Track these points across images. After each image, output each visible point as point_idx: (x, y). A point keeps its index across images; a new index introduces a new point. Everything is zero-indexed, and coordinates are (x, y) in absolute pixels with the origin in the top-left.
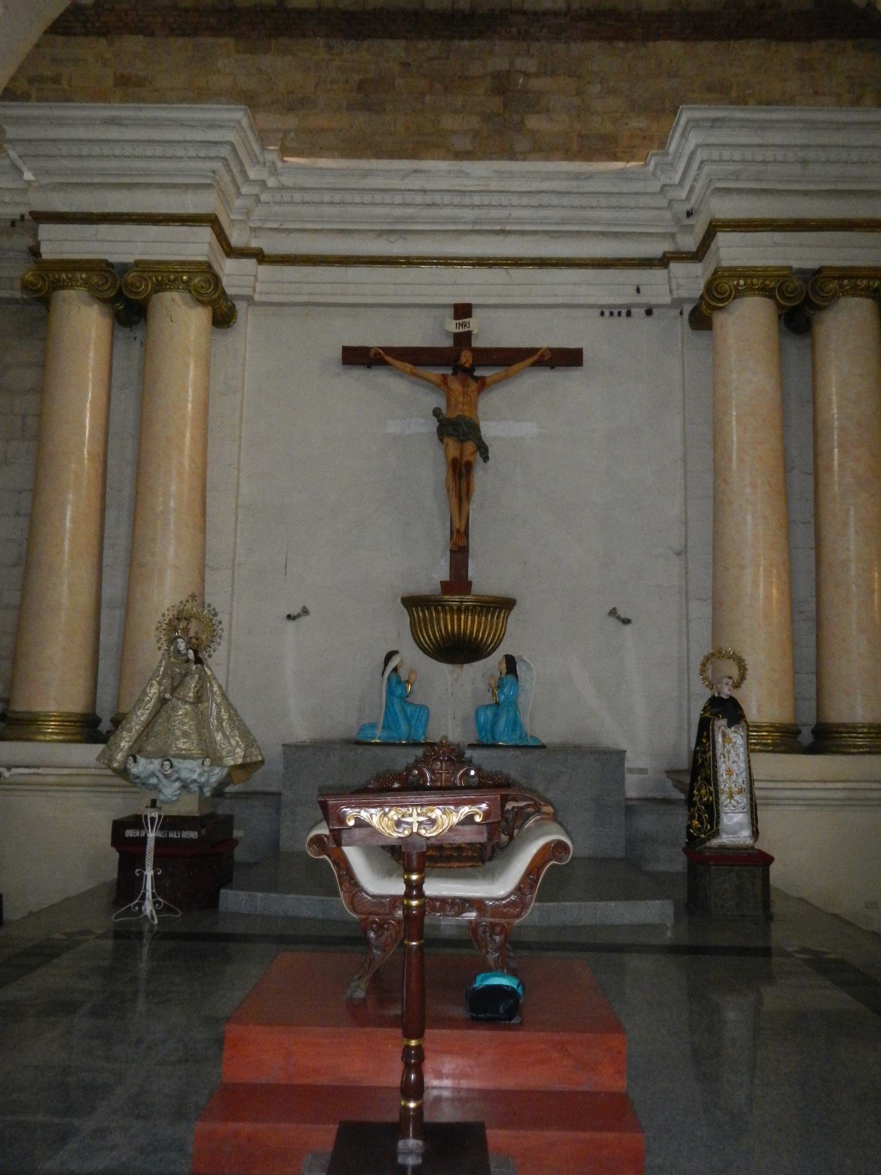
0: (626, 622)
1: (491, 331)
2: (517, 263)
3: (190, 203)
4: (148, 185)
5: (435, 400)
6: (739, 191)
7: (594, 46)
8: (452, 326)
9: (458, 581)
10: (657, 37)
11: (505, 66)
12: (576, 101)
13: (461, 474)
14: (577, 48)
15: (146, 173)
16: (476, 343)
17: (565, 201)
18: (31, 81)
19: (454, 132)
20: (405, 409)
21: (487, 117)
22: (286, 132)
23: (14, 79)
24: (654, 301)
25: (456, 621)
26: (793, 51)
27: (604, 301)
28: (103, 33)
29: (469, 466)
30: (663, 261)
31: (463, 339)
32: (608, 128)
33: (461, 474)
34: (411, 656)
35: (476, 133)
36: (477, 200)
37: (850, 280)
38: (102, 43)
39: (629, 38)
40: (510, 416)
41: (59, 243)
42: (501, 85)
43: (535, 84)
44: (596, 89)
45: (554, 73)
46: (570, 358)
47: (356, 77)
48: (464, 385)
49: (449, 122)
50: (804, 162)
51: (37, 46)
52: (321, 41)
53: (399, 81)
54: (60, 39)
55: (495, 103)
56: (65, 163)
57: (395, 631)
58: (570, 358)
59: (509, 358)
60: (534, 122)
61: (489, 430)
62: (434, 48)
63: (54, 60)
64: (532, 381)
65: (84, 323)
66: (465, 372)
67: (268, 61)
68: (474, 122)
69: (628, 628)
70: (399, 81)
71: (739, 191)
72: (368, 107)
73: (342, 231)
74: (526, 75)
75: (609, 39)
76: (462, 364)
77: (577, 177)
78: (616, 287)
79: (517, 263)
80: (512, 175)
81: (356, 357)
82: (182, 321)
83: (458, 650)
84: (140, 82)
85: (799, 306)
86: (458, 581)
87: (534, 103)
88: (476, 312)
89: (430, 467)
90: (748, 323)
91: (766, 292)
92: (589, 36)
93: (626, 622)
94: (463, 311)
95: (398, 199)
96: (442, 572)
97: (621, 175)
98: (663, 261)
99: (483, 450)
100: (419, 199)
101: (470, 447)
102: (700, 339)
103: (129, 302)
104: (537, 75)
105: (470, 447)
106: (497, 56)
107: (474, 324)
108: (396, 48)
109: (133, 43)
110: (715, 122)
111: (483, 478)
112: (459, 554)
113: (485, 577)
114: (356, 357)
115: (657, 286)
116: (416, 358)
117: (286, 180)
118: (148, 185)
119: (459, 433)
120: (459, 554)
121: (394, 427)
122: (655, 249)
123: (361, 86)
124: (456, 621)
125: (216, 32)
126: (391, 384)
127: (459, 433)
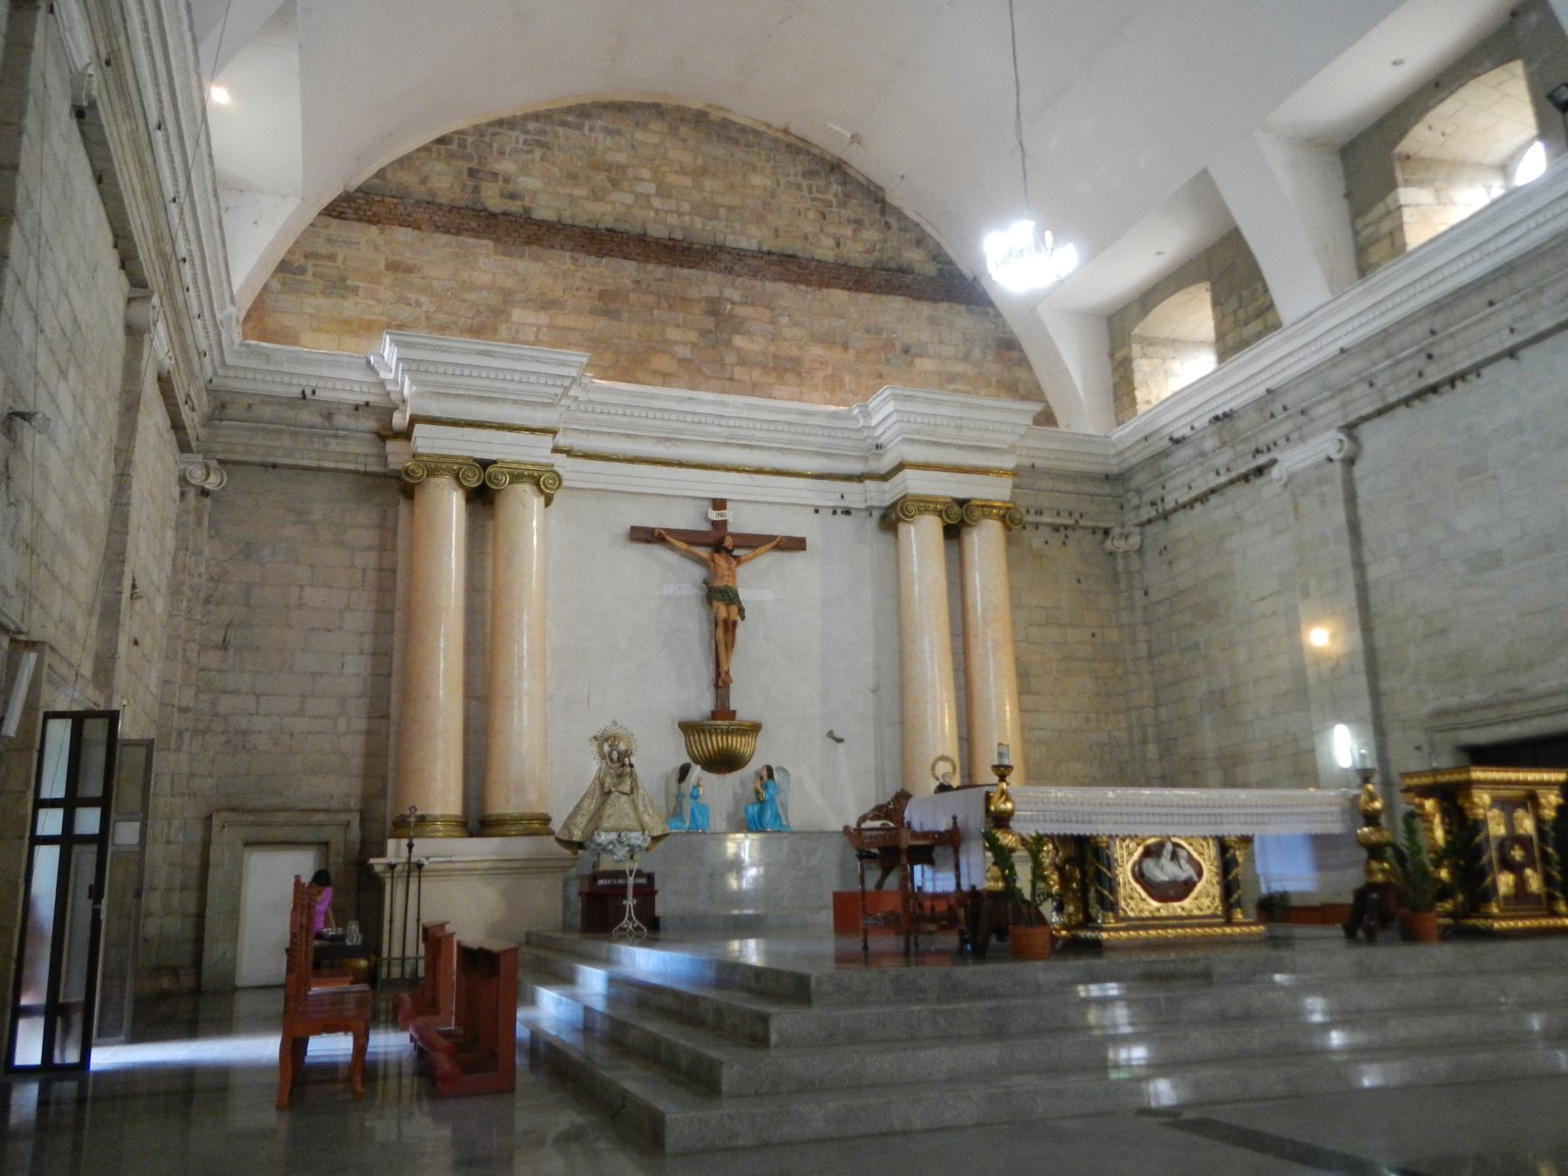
0: (840, 741)
1: (740, 521)
2: (759, 471)
3: (539, 418)
4: (505, 400)
5: (697, 573)
6: (919, 442)
7: (783, 287)
8: (714, 515)
9: (723, 711)
10: (828, 286)
11: (717, 294)
12: (771, 328)
14: (770, 286)
15: (504, 390)
16: (730, 529)
17: (793, 429)
18: (306, 256)
19: (678, 343)
20: (679, 579)
21: (704, 333)
22: (539, 327)
23: (289, 252)
24: (852, 505)
25: (717, 741)
26: (925, 308)
27: (817, 503)
28: (374, 220)
29: (735, 624)
30: (860, 478)
31: (720, 525)
32: (795, 352)
35: (694, 345)
36: (731, 423)
37: (986, 508)
38: (374, 230)
39: (808, 283)
41: (427, 440)
42: (714, 308)
43: (740, 311)
44: (785, 320)
45: (753, 304)
46: (797, 544)
47: (597, 288)
48: (728, 561)
49: (673, 334)
50: (961, 427)
51: (312, 225)
52: (568, 254)
53: (632, 296)
54: (335, 222)
55: (709, 323)
56: (440, 378)
58: (797, 544)
59: (754, 542)
60: (738, 341)
61: (744, 595)
63: (329, 240)
64: (767, 560)
65: (451, 505)
66: (718, 547)
67: (523, 265)
68: (693, 336)
69: (840, 745)
70: (632, 296)
71: (919, 442)
72: (608, 314)
73: (629, 436)
74: (733, 303)
75: (795, 282)
76: (717, 544)
77: (803, 413)
78: (828, 494)
79: (759, 471)
80: (758, 408)
81: (645, 536)
83: (725, 762)
84: (409, 270)
87: (738, 326)
88: (729, 505)
89: (694, 625)
90: (923, 535)
91: (940, 514)
92: (779, 278)
93: (840, 741)
94: (719, 504)
95: (674, 417)
97: (834, 415)
98: (860, 478)
99: (741, 611)
100: (689, 418)
101: (734, 609)
102: (888, 537)
104: (741, 304)
105: (734, 609)
106: (707, 284)
107: (729, 514)
108: (629, 269)
109: (402, 234)
110: (907, 398)
114: (645, 536)
115: (855, 495)
116: (690, 538)
117: (592, 396)
118: (505, 400)
119: (721, 601)
121: (668, 590)
122: (856, 467)
123: (602, 295)
124: (717, 741)
125: (476, 233)
127: (721, 601)
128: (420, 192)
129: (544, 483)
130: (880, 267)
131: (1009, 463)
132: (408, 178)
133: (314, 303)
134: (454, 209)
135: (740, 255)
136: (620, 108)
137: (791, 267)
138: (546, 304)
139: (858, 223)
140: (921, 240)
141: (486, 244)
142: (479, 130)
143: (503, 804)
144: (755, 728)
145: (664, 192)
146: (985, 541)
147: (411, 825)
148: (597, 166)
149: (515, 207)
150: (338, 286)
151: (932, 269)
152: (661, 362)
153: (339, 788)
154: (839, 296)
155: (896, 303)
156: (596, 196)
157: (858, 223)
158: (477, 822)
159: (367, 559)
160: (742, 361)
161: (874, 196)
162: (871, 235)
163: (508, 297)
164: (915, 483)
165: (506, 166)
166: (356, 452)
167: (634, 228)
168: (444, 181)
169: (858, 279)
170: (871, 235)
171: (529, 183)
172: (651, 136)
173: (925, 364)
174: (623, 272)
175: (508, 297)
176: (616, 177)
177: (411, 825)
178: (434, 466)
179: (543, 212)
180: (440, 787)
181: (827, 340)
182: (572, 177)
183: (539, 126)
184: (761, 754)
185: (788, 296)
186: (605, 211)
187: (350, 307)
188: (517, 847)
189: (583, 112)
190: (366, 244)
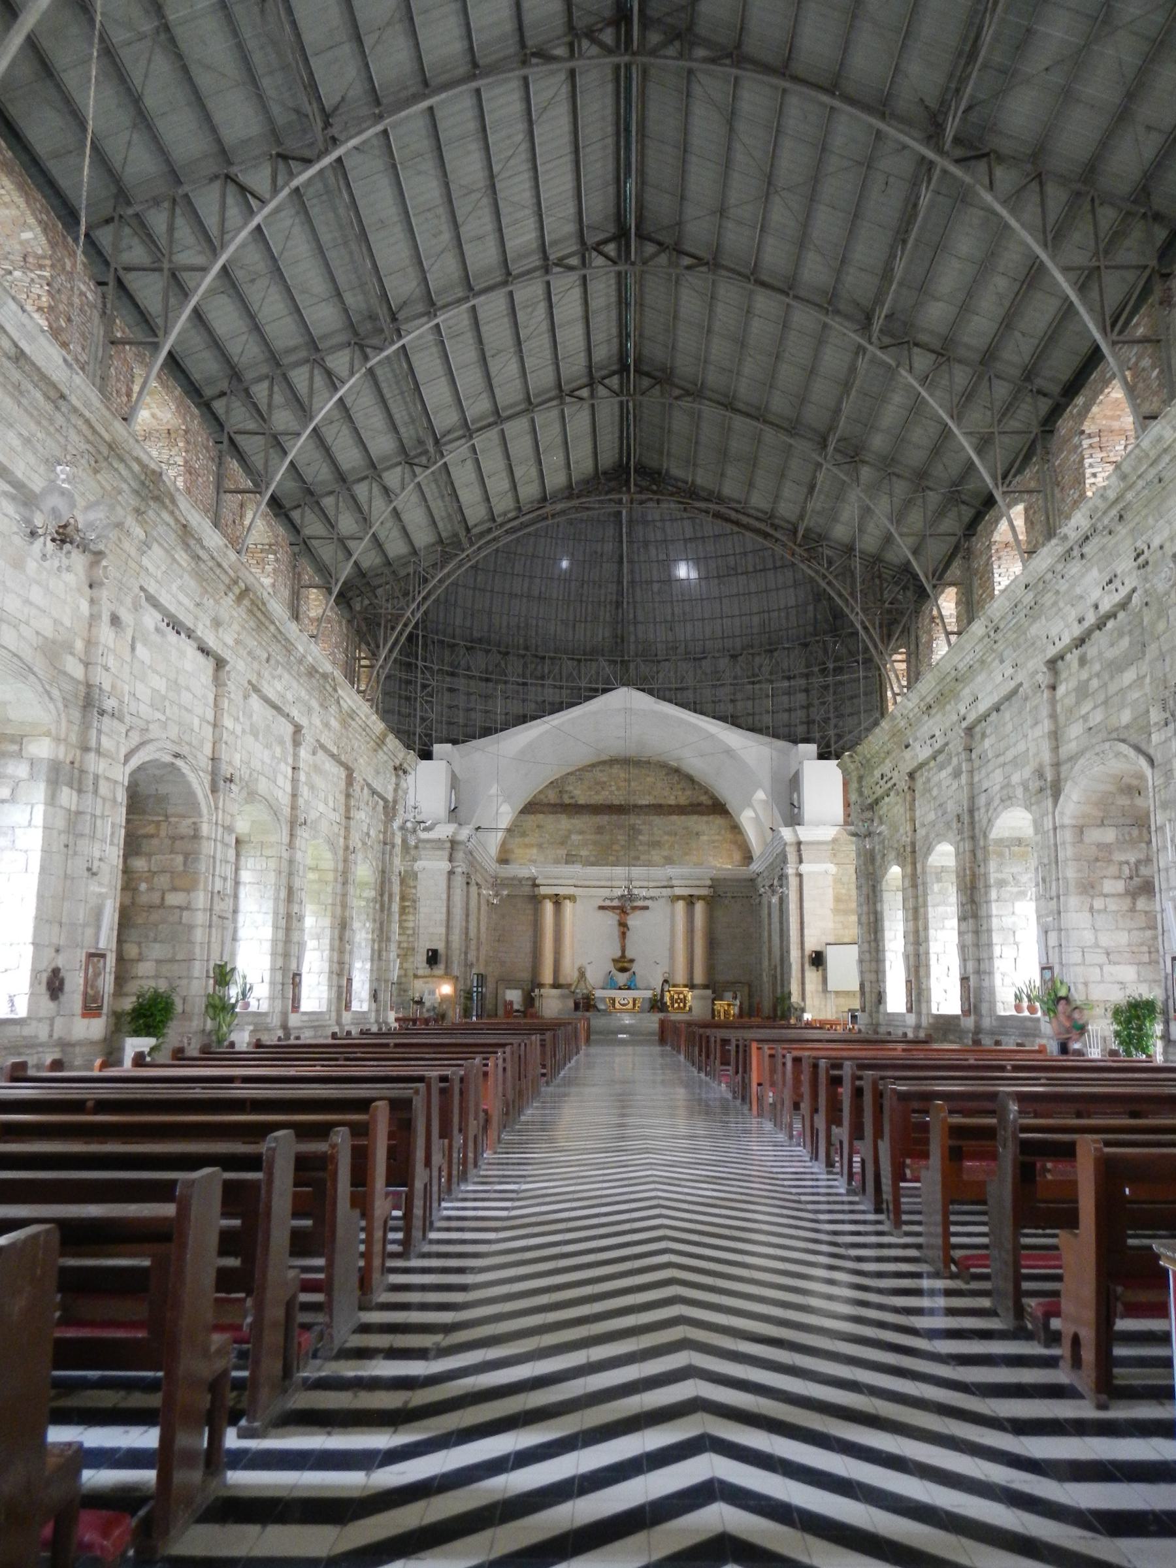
9: (623, 956)
13: (624, 934)
20: (611, 919)
25: (623, 964)
26: (705, 818)
33: (624, 934)
34: (614, 972)
37: (699, 898)
40: (634, 920)
41: (544, 890)
42: (632, 827)
57: (610, 966)
58: (646, 908)
62: (615, 817)
65: (549, 907)
81: (601, 908)
82: (568, 906)
83: (623, 970)
85: (690, 900)
86: (623, 956)
87: (640, 832)
89: (616, 931)
90: (681, 905)
96: (619, 954)
103: (557, 900)
108: (606, 818)
111: (628, 934)
112: (623, 951)
113: (629, 954)
114: (601, 908)
116: (614, 908)
119: (623, 925)
120: (623, 951)
124: (623, 964)
126: (610, 913)
127: (623, 925)
128: (545, 801)
129: (572, 898)
130: (691, 805)
131: (709, 883)
132: (542, 796)
133: (518, 840)
134: (555, 805)
135: (641, 807)
136: (604, 763)
137: (659, 809)
138: (581, 833)
139: (684, 789)
140: (707, 792)
141: (564, 816)
142: (562, 778)
143: (562, 981)
144: (632, 961)
145: (618, 789)
146: (699, 907)
147: (541, 986)
148: (597, 783)
149: (572, 801)
150: (524, 834)
151: (710, 802)
152: (616, 847)
153: (526, 975)
154: (674, 818)
155: (695, 817)
156: (597, 793)
157: (684, 789)
158: (556, 985)
159: (531, 918)
160: (641, 843)
161: (690, 779)
162: (689, 793)
163: (570, 832)
164: (678, 891)
165: (570, 788)
166: (527, 890)
167: (608, 802)
168: (552, 797)
169: (680, 810)
170: (689, 793)
171: (577, 792)
172: (616, 770)
173: (705, 838)
174: (603, 820)
175: (570, 832)
176: (603, 785)
177: (541, 986)
178: (545, 897)
179: (581, 802)
180: (547, 977)
181: (669, 834)
182: (590, 788)
183: (580, 773)
184: (635, 967)
185: (657, 820)
186: (598, 798)
187: (527, 840)
188: (566, 991)
189: (593, 766)
190: (531, 820)
